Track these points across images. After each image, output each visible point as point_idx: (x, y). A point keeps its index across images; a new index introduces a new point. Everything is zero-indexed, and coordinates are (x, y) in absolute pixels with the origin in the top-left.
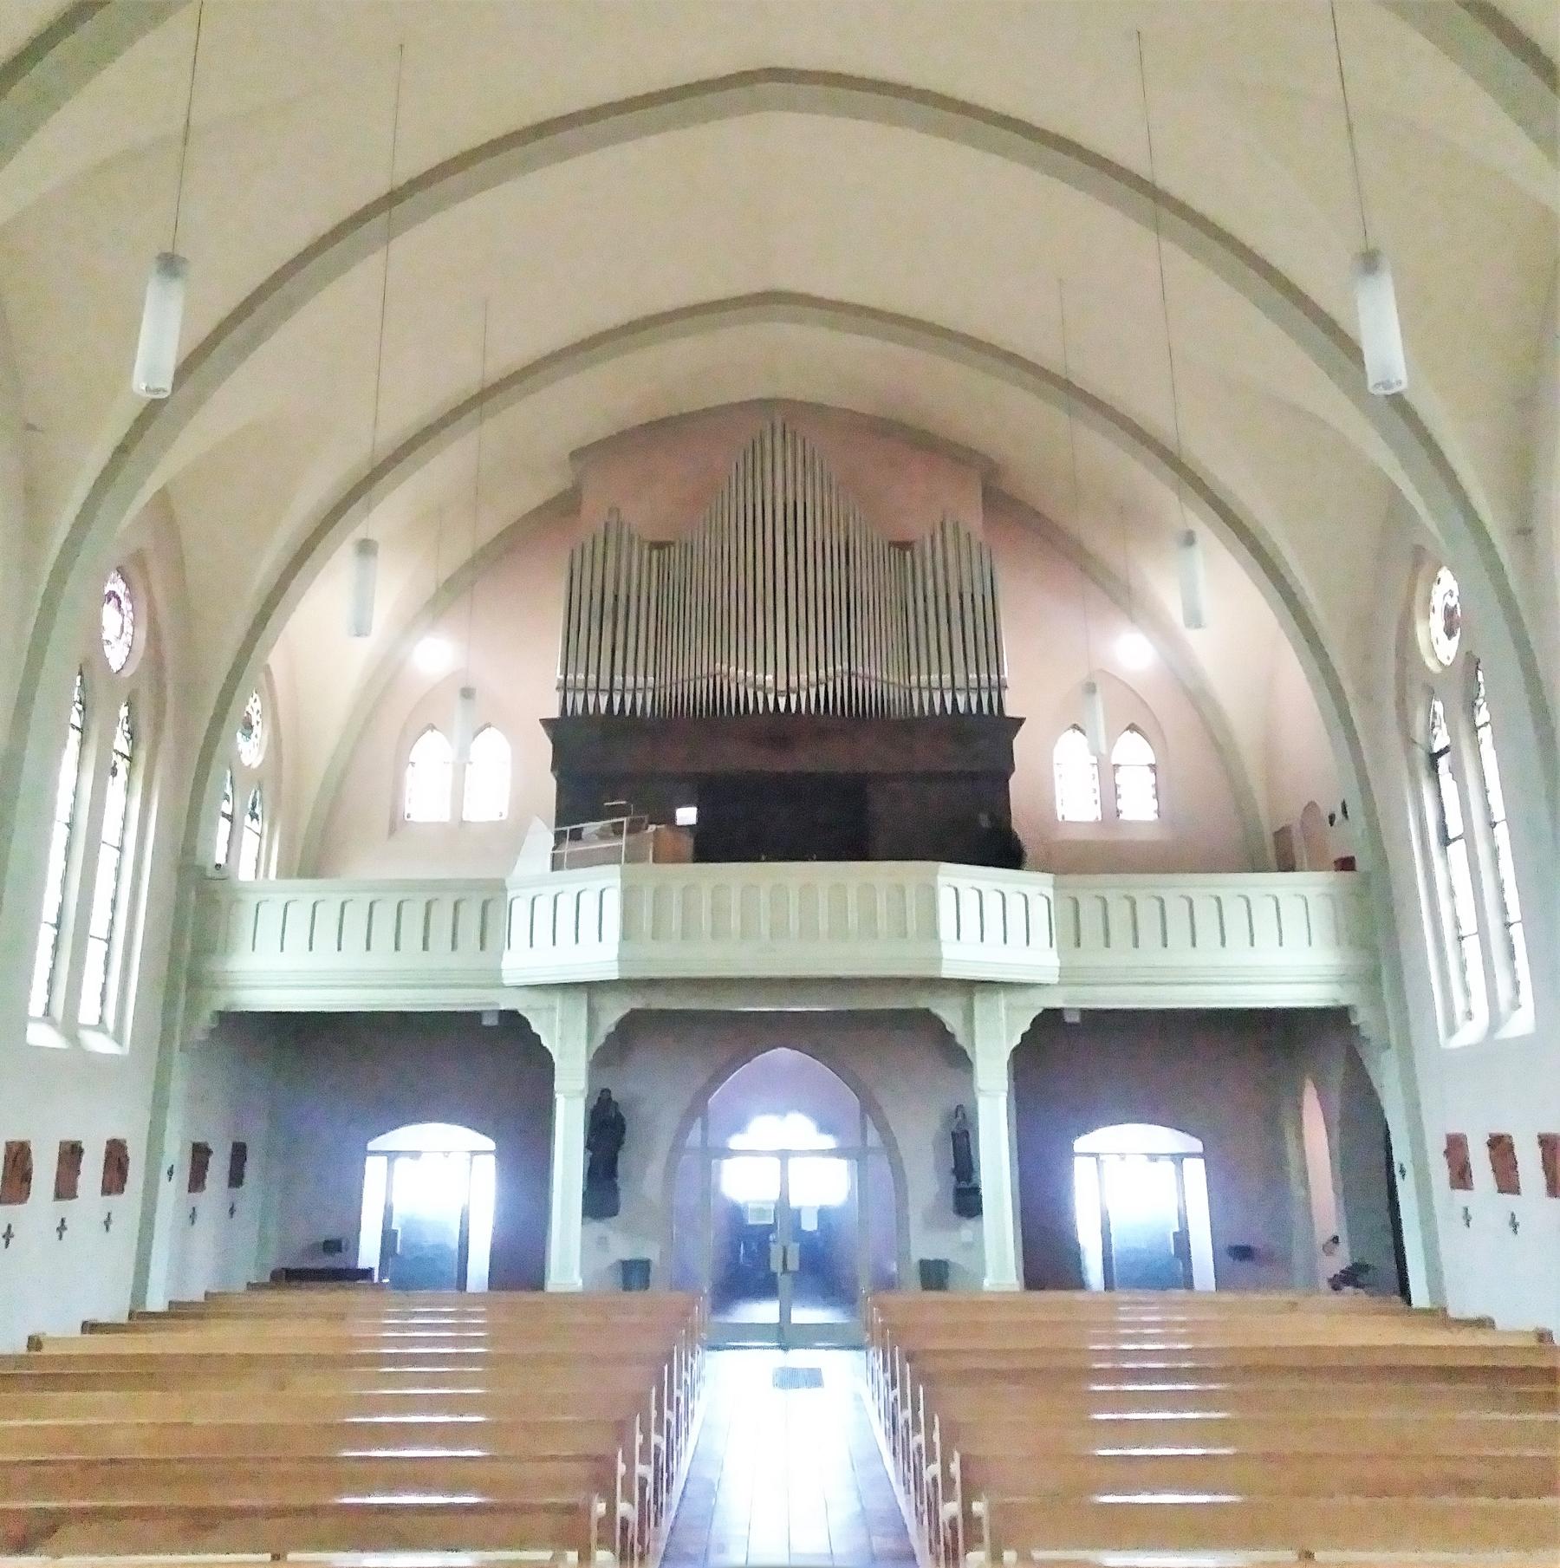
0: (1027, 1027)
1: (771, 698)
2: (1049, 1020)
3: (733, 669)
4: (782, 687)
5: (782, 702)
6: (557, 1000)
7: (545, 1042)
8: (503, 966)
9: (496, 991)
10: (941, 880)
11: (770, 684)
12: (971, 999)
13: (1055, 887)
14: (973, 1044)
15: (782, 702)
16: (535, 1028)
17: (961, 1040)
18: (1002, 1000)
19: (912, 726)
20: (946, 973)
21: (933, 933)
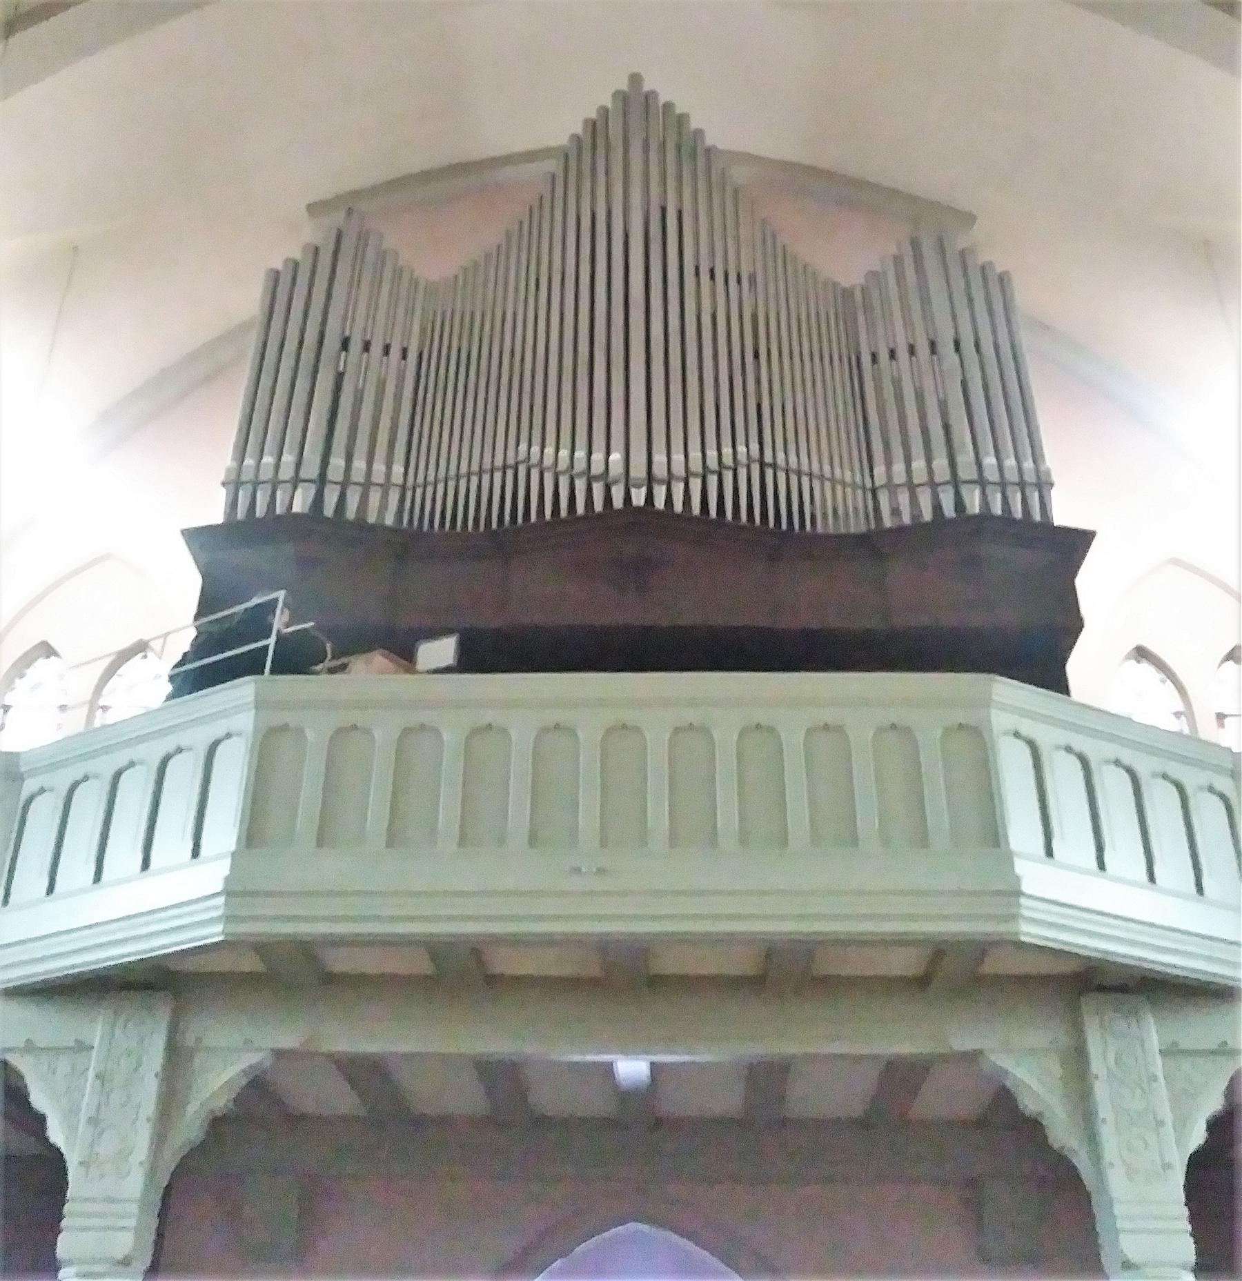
10: (1000, 721)
12: (1078, 1030)
14: (1092, 1139)
17: (1062, 1132)
18: (1152, 1031)
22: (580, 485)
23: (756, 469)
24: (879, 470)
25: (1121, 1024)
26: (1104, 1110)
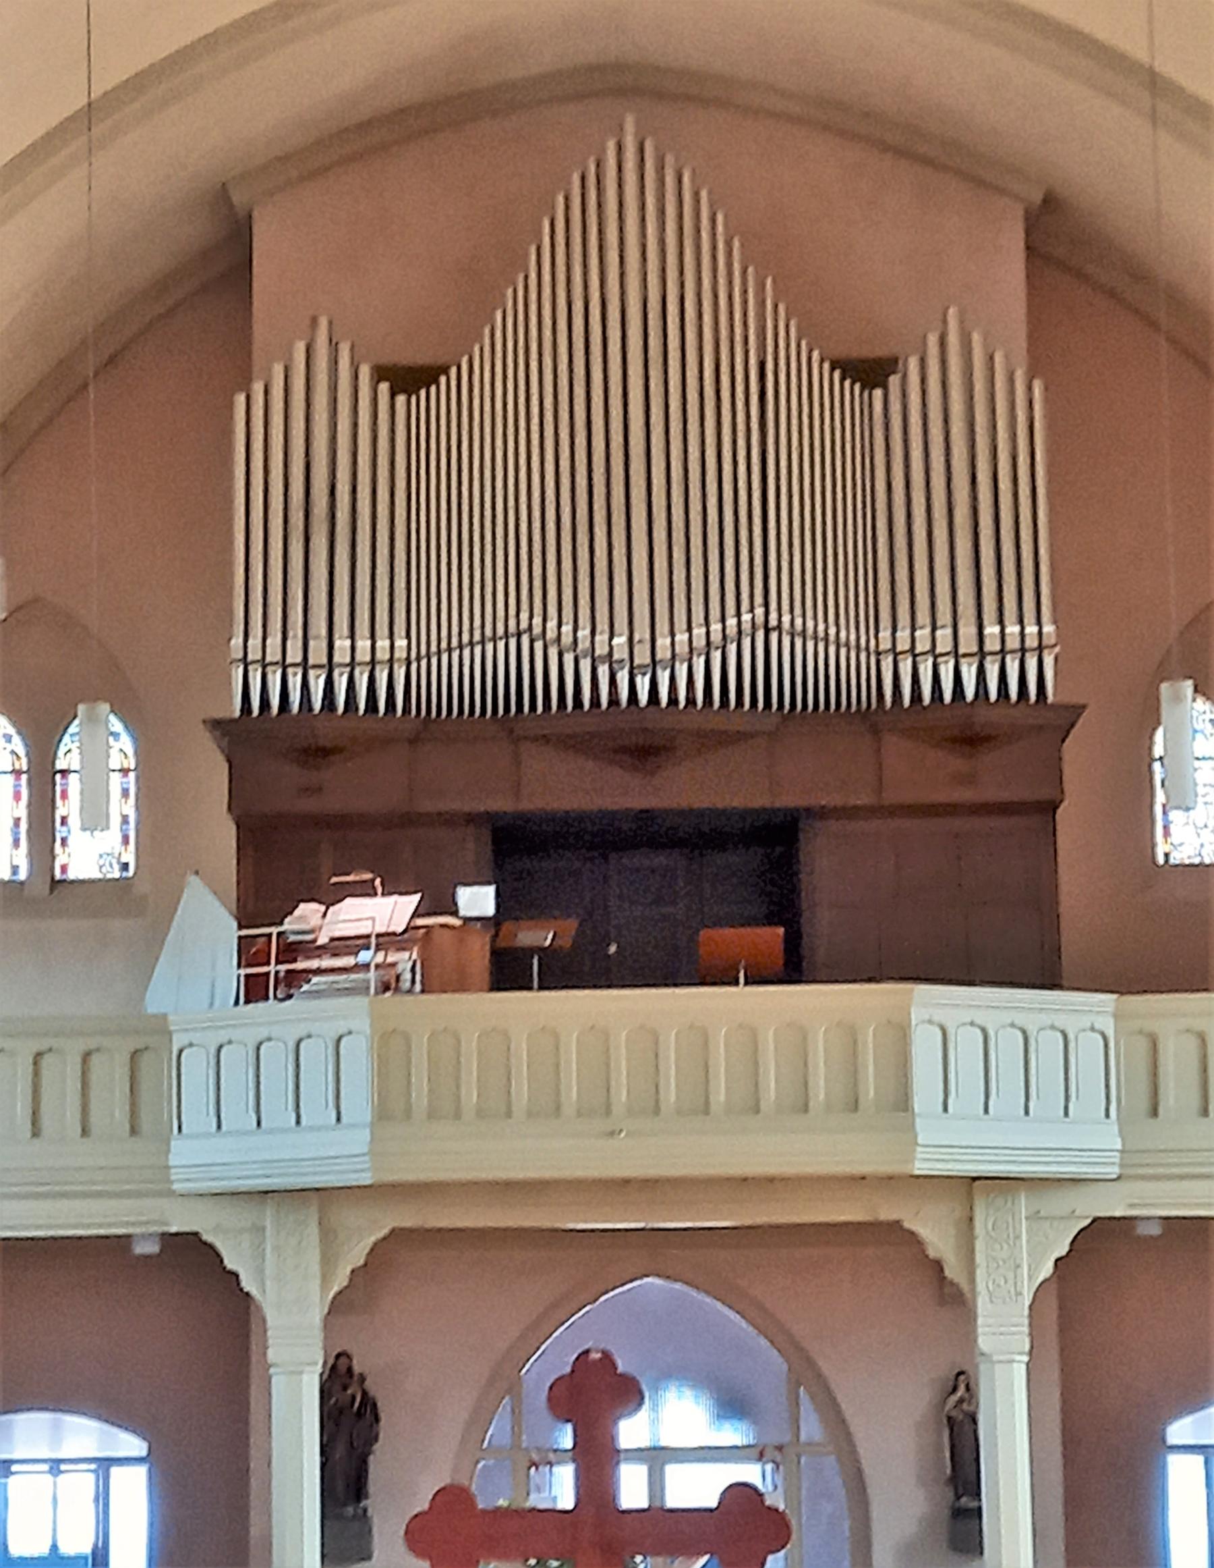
0: (1063, 1250)
1: (623, 678)
2: (1101, 1240)
3: (552, 624)
4: (642, 656)
5: (643, 685)
6: (269, 1216)
7: (247, 1284)
8: (173, 1160)
9: (164, 1202)
11: (621, 653)
13: (1116, 1016)
15: (643, 685)
16: (230, 1264)
18: (1023, 1203)
19: (876, 720)
20: (920, 1167)
21: (903, 1102)
22: (585, 666)
23: (760, 635)
24: (885, 634)
25: (1000, 1201)
26: (980, 1258)
